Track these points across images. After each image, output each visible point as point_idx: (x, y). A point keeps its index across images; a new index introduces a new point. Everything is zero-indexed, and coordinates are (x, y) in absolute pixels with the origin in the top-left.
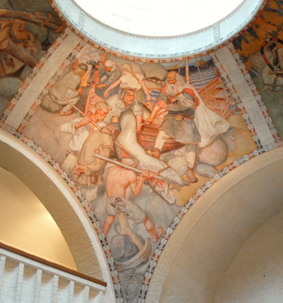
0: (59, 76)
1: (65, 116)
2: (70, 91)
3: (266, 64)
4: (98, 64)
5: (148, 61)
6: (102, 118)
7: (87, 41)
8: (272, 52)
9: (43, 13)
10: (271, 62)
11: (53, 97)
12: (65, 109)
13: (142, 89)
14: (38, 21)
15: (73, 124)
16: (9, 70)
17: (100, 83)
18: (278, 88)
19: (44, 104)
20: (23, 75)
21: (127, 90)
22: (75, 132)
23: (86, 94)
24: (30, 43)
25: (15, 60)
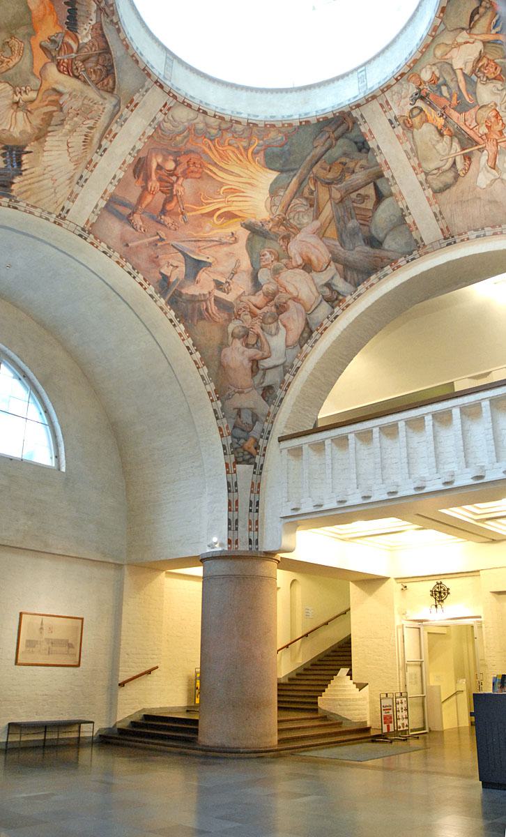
0: (412, 149)
1: (469, 169)
2: (439, 146)
4: (420, 90)
5: (442, 15)
6: (500, 124)
7: (381, 92)
9: (320, 136)
11: (435, 172)
12: (460, 166)
13: (485, 43)
14: (327, 145)
15: (486, 168)
16: (369, 204)
17: (450, 100)
19: (436, 187)
20: (385, 191)
21: (476, 66)
22: (498, 172)
23: (456, 127)
24: (351, 165)
25: (362, 192)
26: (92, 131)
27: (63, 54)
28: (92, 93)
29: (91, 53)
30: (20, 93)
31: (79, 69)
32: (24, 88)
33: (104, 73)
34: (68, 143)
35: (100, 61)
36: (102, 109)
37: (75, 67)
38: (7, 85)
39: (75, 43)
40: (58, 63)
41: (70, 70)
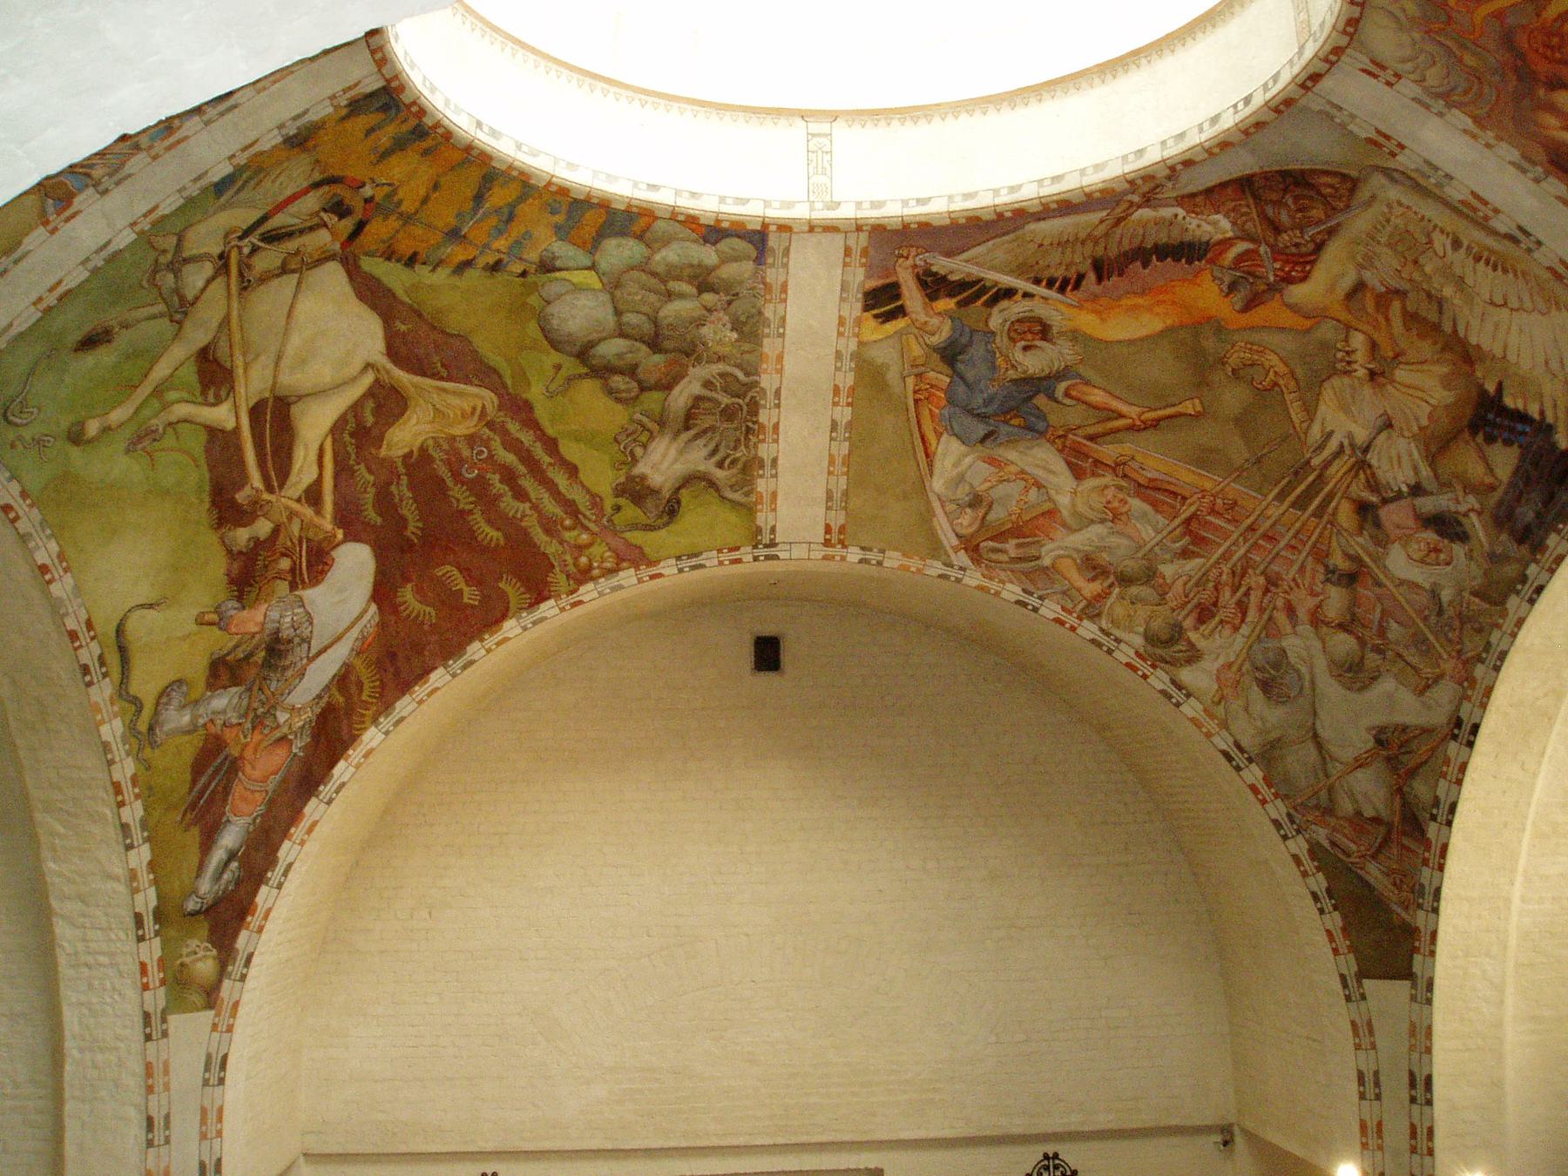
10: (278, 221)
18: (169, 279)
26: (1466, 243)
28: (1359, 222)
29: (1255, 216)
30: (1349, 363)
31: (1298, 240)
32: (1340, 355)
33: (1298, 191)
34: (1492, 303)
35: (1274, 196)
36: (1401, 210)
37: (1294, 250)
38: (1326, 385)
39: (1231, 245)
40: (1283, 280)
41: (1301, 263)
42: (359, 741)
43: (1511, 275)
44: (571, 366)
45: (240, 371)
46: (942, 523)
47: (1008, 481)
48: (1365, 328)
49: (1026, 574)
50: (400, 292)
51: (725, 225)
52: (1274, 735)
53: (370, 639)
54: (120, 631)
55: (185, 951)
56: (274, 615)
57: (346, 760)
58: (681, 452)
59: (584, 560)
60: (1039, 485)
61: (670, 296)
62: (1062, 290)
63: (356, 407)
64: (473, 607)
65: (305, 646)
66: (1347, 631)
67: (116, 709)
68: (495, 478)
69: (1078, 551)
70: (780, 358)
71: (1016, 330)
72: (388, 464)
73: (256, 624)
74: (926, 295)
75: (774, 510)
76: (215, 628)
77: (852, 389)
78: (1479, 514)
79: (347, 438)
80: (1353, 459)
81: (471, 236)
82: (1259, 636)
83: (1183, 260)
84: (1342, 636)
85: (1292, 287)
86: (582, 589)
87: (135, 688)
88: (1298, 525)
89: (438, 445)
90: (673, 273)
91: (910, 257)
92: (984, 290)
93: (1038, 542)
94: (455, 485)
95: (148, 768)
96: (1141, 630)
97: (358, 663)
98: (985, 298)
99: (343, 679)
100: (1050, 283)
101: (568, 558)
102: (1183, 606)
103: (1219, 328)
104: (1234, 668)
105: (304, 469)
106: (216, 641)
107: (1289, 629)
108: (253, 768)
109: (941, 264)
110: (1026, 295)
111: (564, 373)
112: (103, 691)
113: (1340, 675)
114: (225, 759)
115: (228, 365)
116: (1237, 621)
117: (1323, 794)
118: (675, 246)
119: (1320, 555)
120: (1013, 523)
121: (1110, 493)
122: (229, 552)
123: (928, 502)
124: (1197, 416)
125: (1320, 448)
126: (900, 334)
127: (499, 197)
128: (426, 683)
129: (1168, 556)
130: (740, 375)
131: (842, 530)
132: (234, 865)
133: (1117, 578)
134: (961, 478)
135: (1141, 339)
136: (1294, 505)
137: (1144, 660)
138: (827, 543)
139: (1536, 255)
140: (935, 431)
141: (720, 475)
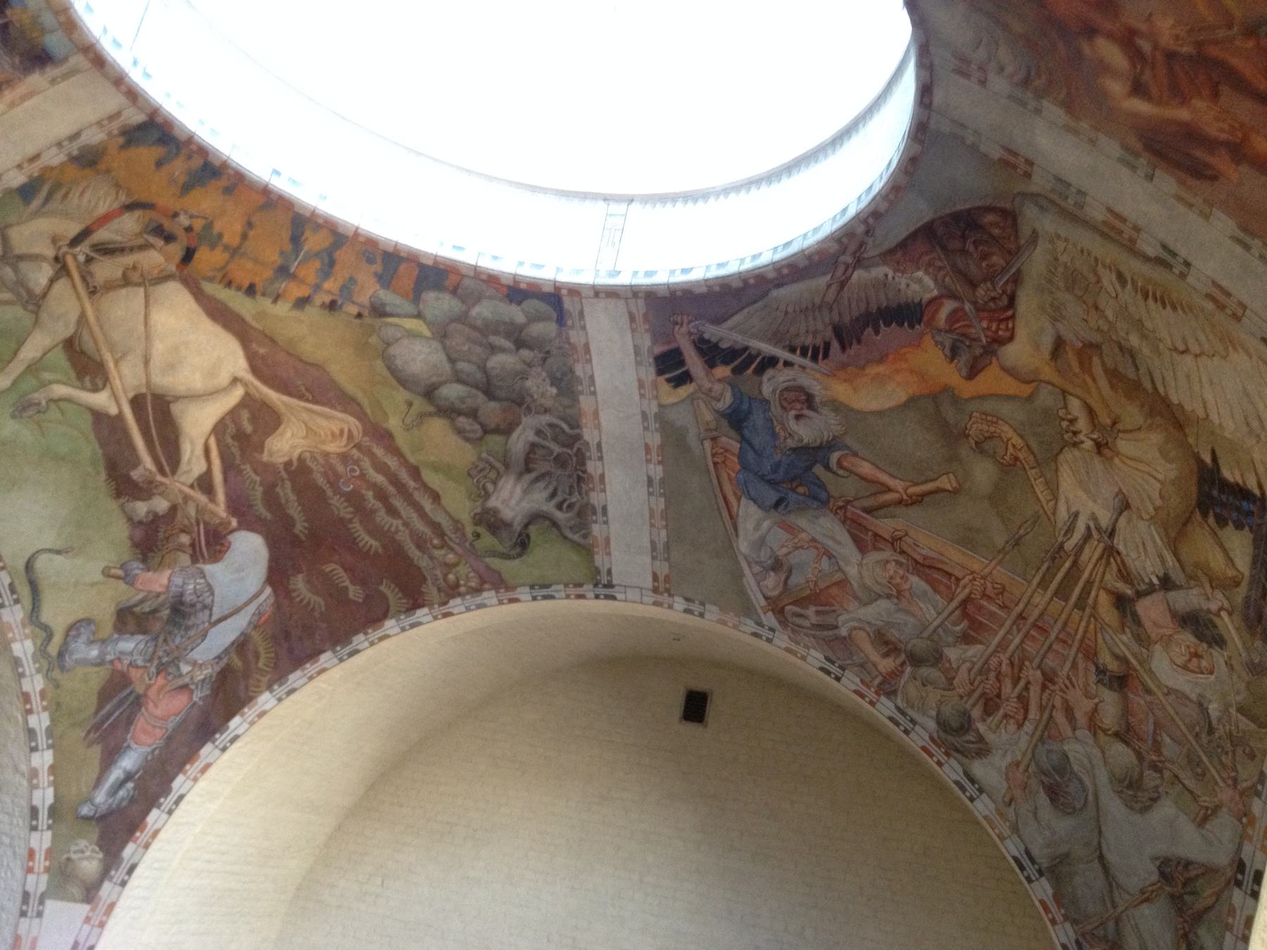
3: (88, 222)
8: (140, 233)
10: (102, 235)
27: (973, 331)
28: (1036, 263)
29: (948, 268)
31: (993, 294)
32: (1065, 424)
37: (992, 304)
38: (1061, 457)
39: (941, 305)
42: (254, 701)
43: (1180, 312)
44: (419, 404)
45: (111, 365)
46: (750, 581)
47: (802, 547)
48: (1078, 391)
49: (828, 642)
50: (249, 318)
51: (523, 286)
52: (1063, 849)
53: (266, 616)
54: (29, 566)
55: (73, 848)
56: (178, 580)
57: (242, 716)
58: (525, 492)
59: (451, 577)
60: (830, 556)
61: (493, 349)
62: (815, 358)
63: (233, 413)
64: (356, 603)
65: (207, 612)
66: (1127, 743)
67: (27, 631)
68: (369, 495)
69: (869, 623)
70: (596, 414)
71: (786, 399)
72: (268, 468)
73: (160, 585)
74: (705, 361)
75: (609, 554)
76: (121, 582)
77: (661, 447)
78: (1230, 614)
79: (229, 440)
80: (1102, 545)
81: (302, 274)
82: (1042, 736)
83: (906, 324)
84: (1120, 747)
85: (1004, 348)
86: (452, 603)
87: (46, 616)
88: (1064, 616)
89: (314, 458)
90: (489, 328)
91: (684, 325)
92: (751, 359)
93: (834, 611)
94: (335, 494)
95: (57, 686)
96: (934, 713)
97: (256, 636)
98: (753, 366)
99: (241, 645)
100: (804, 353)
101: (438, 572)
102: (970, 694)
103: (956, 400)
104: (1022, 768)
105: (193, 461)
106: (119, 593)
107: (1069, 732)
108: (156, 706)
109: (712, 332)
110: (787, 364)
111: (414, 407)
112: (15, 615)
113: (1122, 792)
114: (131, 692)
115: (99, 359)
116: (1020, 717)
117: (1111, 925)
118: (485, 303)
119: (1090, 654)
120: (811, 590)
121: (891, 567)
122: (130, 519)
123: (738, 563)
124: (956, 492)
125: (1070, 530)
126: (692, 398)
127: (314, 242)
128: (316, 662)
129: (950, 639)
130: (565, 426)
131: (667, 579)
132: (130, 785)
133: (907, 656)
134: (762, 542)
135: (891, 410)
136: (1056, 594)
137: (939, 747)
138: (655, 590)
139: (1190, 279)
140: (735, 494)
141: (560, 516)
